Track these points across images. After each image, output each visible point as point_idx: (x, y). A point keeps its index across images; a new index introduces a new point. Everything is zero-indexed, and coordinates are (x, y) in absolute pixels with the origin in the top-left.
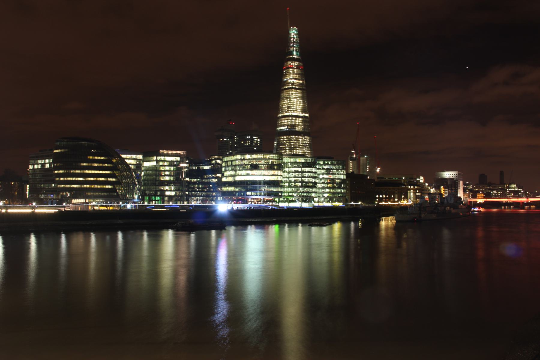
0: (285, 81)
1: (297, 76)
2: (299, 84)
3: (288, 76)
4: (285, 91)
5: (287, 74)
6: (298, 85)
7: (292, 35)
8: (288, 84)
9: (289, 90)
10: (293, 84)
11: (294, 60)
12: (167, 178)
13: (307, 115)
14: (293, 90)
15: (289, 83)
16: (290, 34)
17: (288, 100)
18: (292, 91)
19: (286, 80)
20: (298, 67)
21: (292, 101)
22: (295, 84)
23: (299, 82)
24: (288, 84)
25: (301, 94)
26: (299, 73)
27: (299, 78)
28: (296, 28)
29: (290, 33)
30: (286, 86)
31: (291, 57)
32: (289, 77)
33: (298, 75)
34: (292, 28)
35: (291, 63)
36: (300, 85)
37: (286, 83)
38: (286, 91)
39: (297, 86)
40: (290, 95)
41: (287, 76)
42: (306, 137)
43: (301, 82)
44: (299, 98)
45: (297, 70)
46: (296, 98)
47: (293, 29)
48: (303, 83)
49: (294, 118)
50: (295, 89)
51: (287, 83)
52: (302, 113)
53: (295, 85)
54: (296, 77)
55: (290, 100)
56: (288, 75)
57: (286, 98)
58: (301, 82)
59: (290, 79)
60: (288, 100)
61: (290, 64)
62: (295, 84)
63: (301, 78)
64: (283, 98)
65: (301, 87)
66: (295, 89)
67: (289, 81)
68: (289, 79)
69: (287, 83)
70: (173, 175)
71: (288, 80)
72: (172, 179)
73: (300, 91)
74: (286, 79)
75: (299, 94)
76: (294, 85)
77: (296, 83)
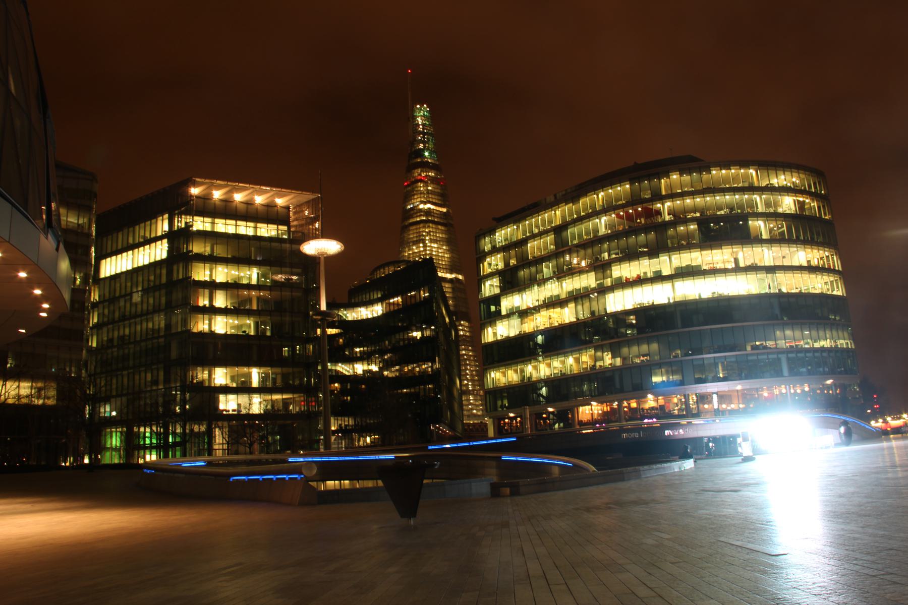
0: (412, 209)
1: (436, 197)
2: (440, 214)
3: (418, 198)
4: (411, 228)
5: (414, 195)
6: (438, 216)
7: (420, 120)
8: (419, 214)
9: (422, 225)
10: (428, 212)
11: (425, 166)
12: (221, 325)
13: (460, 277)
14: (431, 225)
15: (421, 210)
16: (414, 118)
17: (421, 245)
18: (429, 227)
19: (411, 206)
20: (433, 180)
21: (428, 248)
22: (432, 214)
23: (440, 209)
25: (445, 234)
26: (439, 193)
27: (440, 202)
29: (415, 116)
30: (413, 218)
31: (419, 160)
32: (419, 200)
33: (438, 195)
34: (418, 106)
35: (421, 171)
36: (442, 217)
37: (412, 212)
38: (414, 227)
39: (437, 217)
40: (423, 236)
41: (414, 199)
42: (462, 322)
43: (444, 210)
44: (443, 241)
45: (435, 186)
46: (435, 241)
48: (448, 211)
50: (433, 222)
51: (415, 211)
52: (451, 273)
53: (434, 216)
54: (434, 201)
55: (425, 246)
56: (416, 197)
57: (416, 241)
58: (444, 210)
59: (422, 202)
60: (421, 245)
61: (420, 175)
62: (434, 213)
63: (443, 203)
64: (409, 243)
65: (445, 221)
66: (433, 222)
67: (421, 206)
68: (420, 204)
69: (416, 211)
70: (255, 307)
71: (418, 205)
72: (249, 325)
73: (443, 228)
74: (413, 204)
75: (442, 233)
76: (431, 216)
77: (435, 211)
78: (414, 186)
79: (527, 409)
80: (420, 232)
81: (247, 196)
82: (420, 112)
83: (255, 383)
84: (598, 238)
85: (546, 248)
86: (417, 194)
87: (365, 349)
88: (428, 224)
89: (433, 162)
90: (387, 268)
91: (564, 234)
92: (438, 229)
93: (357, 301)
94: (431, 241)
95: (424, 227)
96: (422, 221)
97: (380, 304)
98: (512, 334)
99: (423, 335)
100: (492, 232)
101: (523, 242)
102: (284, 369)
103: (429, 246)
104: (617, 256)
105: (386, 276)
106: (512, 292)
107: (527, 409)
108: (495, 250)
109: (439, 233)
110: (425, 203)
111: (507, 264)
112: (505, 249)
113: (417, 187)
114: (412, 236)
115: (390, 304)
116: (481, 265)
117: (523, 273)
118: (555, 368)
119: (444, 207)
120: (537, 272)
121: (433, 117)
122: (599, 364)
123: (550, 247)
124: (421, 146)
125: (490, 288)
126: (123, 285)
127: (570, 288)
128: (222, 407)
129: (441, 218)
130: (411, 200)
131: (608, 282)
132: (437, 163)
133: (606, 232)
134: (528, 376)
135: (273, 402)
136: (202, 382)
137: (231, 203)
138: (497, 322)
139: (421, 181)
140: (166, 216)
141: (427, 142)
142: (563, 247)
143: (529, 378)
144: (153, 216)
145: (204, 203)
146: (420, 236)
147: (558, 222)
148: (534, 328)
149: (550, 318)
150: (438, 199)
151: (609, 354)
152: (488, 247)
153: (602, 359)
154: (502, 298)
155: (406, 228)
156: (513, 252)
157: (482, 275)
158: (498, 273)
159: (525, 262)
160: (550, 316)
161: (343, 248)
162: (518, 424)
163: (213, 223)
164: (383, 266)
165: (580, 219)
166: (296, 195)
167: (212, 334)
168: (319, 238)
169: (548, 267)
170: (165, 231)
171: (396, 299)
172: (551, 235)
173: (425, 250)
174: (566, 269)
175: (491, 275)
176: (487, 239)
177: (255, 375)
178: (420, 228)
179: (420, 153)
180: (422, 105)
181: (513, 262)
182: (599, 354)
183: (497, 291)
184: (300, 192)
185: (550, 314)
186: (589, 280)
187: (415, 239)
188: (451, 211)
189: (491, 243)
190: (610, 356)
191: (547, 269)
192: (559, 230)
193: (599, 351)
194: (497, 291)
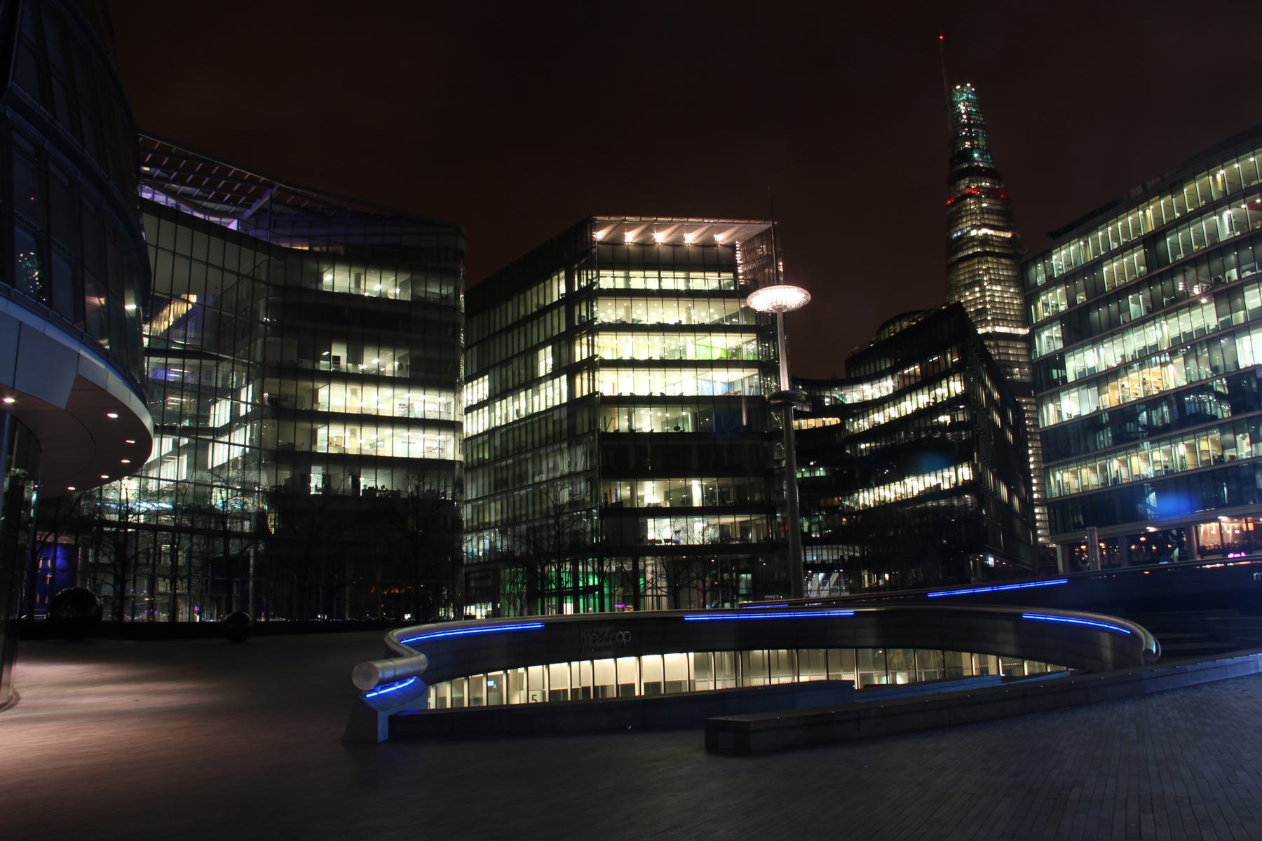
1: (995, 217)
2: (1003, 242)
5: (962, 217)
6: (1000, 245)
7: (962, 108)
8: (971, 244)
9: (976, 260)
10: (985, 240)
11: (976, 173)
14: (989, 259)
16: (954, 105)
17: (977, 289)
18: (987, 262)
19: (959, 234)
20: (989, 193)
22: (991, 243)
23: (1002, 234)
24: (968, 242)
25: (1012, 270)
27: (1001, 224)
28: (972, 86)
29: (955, 102)
31: (966, 166)
32: (969, 223)
34: (958, 87)
35: (970, 182)
37: (961, 243)
38: (965, 264)
39: (998, 246)
40: (979, 275)
41: (962, 223)
43: (1009, 235)
44: (1009, 281)
45: (992, 201)
46: (998, 282)
47: (963, 92)
48: (1013, 236)
49: (1001, 343)
50: (992, 254)
53: (993, 245)
54: (992, 223)
55: (983, 290)
56: (965, 220)
57: (970, 283)
58: (1009, 235)
59: (974, 227)
61: (968, 187)
62: (992, 240)
65: (1010, 252)
66: (992, 254)
67: (974, 233)
68: (972, 229)
69: (966, 240)
71: (969, 232)
73: (1008, 262)
74: (961, 230)
75: (1007, 270)
76: (990, 246)
77: (994, 238)
78: (961, 204)
79: (1094, 530)
80: (974, 270)
81: (670, 235)
82: (962, 96)
83: (697, 501)
84: (1219, 246)
85: (1132, 270)
86: (966, 216)
87: (873, 445)
88: (985, 258)
89: (986, 166)
90: (898, 324)
91: (1160, 246)
92: (1002, 264)
93: (858, 375)
94: (991, 282)
95: (979, 262)
96: (976, 255)
97: (889, 378)
98: (1085, 412)
99: (952, 419)
100: (1047, 254)
101: (1096, 265)
102: (735, 479)
103: (989, 290)
104: (1255, 273)
105: (896, 335)
106: (1083, 346)
107: (1094, 530)
108: (1052, 282)
109: (1002, 269)
110: (979, 228)
111: (1071, 302)
112: (1067, 279)
113: (965, 206)
114: (963, 277)
115: (903, 377)
116: (1032, 307)
117: (1099, 315)
118: (1155, 462)
119: (1008, 232)
120: (1119, 312)
121: (981, 101)
122: (1228, 453)
123: (1139, 268)
124: (968, 144)
125: (1049, 340)
126: (516, 372)
127: (1175, 333)
128: (651, 535)
129: (1004, 247)
130: (958, 225)
131: (1240, 317)
132: (993, 167)
133: (1232, 236)
134: (1113, 477)
135: (722, 527)
136: (620, 503)
137: (653, 247)
138: (1062, 394)
139: (971, 195)
140: (562, 274)
141: (976, 138)
142: (1159, 267)
143: (1116, 480)
144: (546, 275)
145: (613, 250)
146: (974, 276)
147: (1151, 227)
148: (1119, 400)
149: (1144, 384)
150: (998, 221)
151: (1246, 436)
152: (1041, 280)
153: (1234, 445)
154: (1067, 356)
155: (952, 267)
156: (1079, 283)
157: (1034, 322)
158: (1058, 318)
159: (1100, 296)
160: (1144, 379)
161: (809, 297)
162: (1104, 553)
163: (627, 278)
164: (892, 321)
165: (1187, 219)
166: (741, 225)
167: (632, 435)
168: (779, 283)
169: (1136, 302)
170: (562, 295)
171: (912, 369)
172: (1140, 249)
173: (983, 296)
174: (1166, 302)
175: (1048, 322)
176: (1040, 267)
177: (697, 490)
178: (974, 264)
179: (967, 155)
180: (963, 85)
181: (1081, 298)
182: (1229, 437)
183: (1059, 345)
184: (747, 222)
185: (1144, 377)
186: (1205, 317)
187: (967, 282)
188: (1018, 236)
189: (1045, 273)
190: (1248, 440)
191: (1136, 306)
192: (1151, 241)
193: (1229, 433)
194: (1059, 345)
